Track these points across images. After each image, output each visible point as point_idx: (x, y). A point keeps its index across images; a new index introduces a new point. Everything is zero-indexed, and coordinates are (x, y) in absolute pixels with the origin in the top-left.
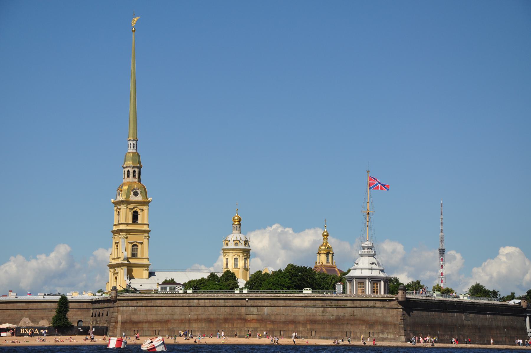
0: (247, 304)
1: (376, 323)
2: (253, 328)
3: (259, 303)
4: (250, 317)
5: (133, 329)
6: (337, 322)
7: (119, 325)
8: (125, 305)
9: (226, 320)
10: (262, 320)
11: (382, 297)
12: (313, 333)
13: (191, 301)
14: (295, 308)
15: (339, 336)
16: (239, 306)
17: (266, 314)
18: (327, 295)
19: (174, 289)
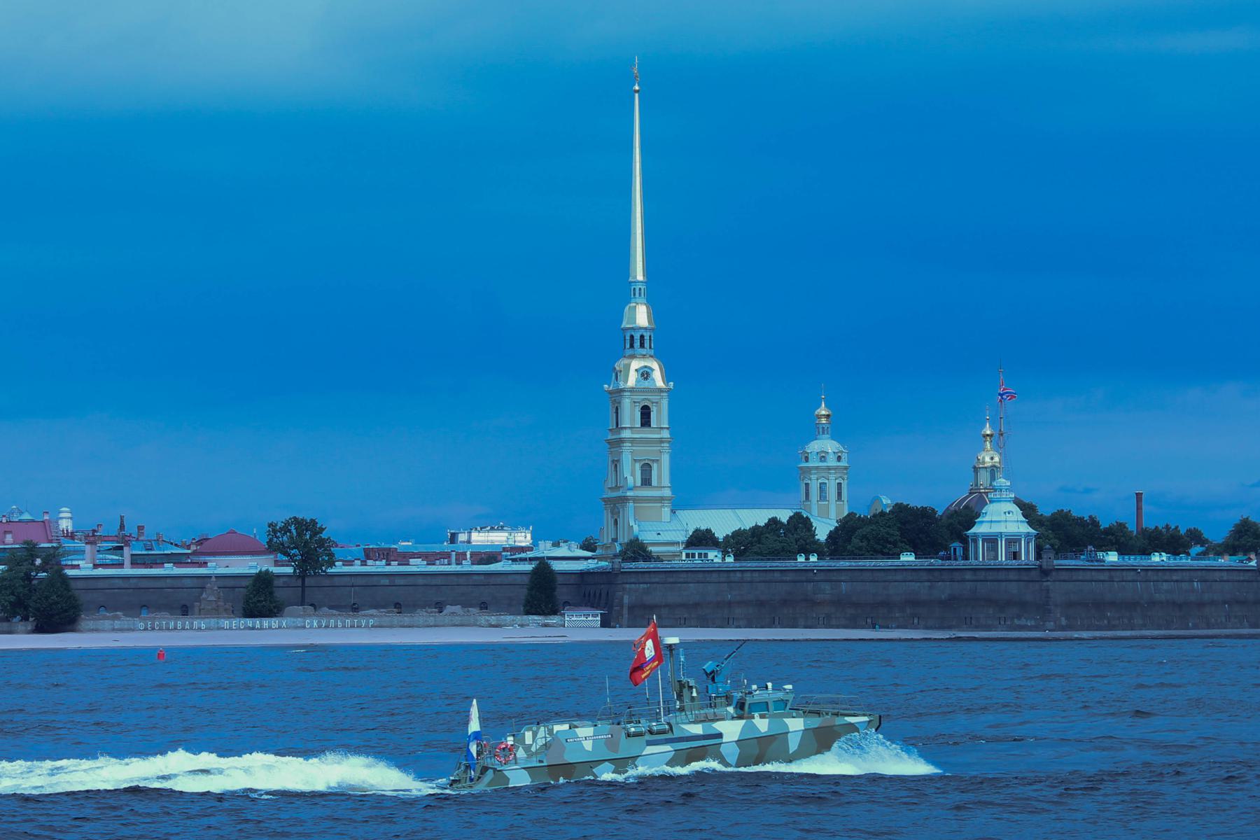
0: (816, 578)
2: (826, 614)
4: (820, 597)
6: (950, 603)
7: (625, 611)
8: (633, 580)
9: (785, 603)
10: (839, 602)
11: (1018, 565)
12: (916, 621)
13: (732, 574)
14: (887, 583)
15: (954, 623)
16: (803, 582)
17: (844, 592)
18: (935, 563)
19: (706, 555)
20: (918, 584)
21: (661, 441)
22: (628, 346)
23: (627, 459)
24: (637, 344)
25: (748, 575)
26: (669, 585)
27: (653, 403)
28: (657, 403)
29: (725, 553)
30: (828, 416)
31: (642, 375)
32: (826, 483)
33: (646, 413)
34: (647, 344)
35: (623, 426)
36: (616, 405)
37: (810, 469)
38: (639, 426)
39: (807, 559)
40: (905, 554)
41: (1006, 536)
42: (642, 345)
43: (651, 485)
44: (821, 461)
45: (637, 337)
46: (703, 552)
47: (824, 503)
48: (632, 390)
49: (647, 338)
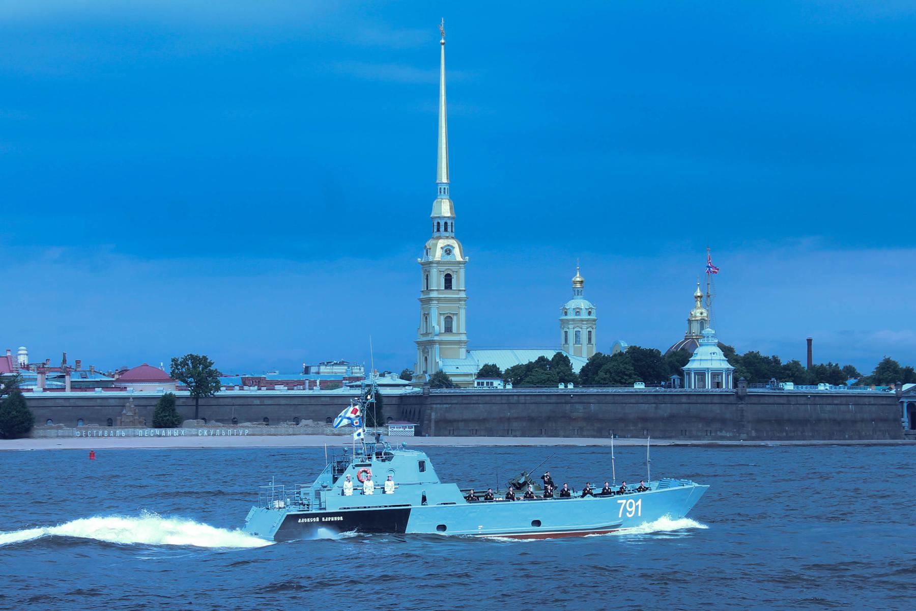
0: (573, 401)
1: (713, 420)
3: (584, 399)
4: (575, 415)
5: (449, 429)
6: (671, 419)
7: (433, 424)
8: (439, 402)
9: (549, 419)
10: (589, 419)
11: (720, 392)
12: (645, 432)
13: (510, 398)
14: (624, 405)
15: (673, 434)
18: (660, 390)
19: (492, 383)
20: (647, 406)
21: (459, 300)
22: (435, 230)
23: (434, 313)
24: (442, 228)
25: (523, 398)
26: (465, 405)
27: (453, 272)
28: (457, 272)
29: (506, 382)
30: (581, 282)
31: (446, 251)
32: (580, 331)
33: (448, 279)
34: (449, 229)
35: (432, 289)
36: (427, 273)
37: (568, 320)
38: (444, 289)
39: (566, 387)
40: (637, 383)
41: (711, 370)
42: (446, 230)
43: (452, 332)
44: (576, 315)
45: (442, 224)
46: (490, 381)
47: (578, 346)
48: (438, 263)
49: (449, 224)
